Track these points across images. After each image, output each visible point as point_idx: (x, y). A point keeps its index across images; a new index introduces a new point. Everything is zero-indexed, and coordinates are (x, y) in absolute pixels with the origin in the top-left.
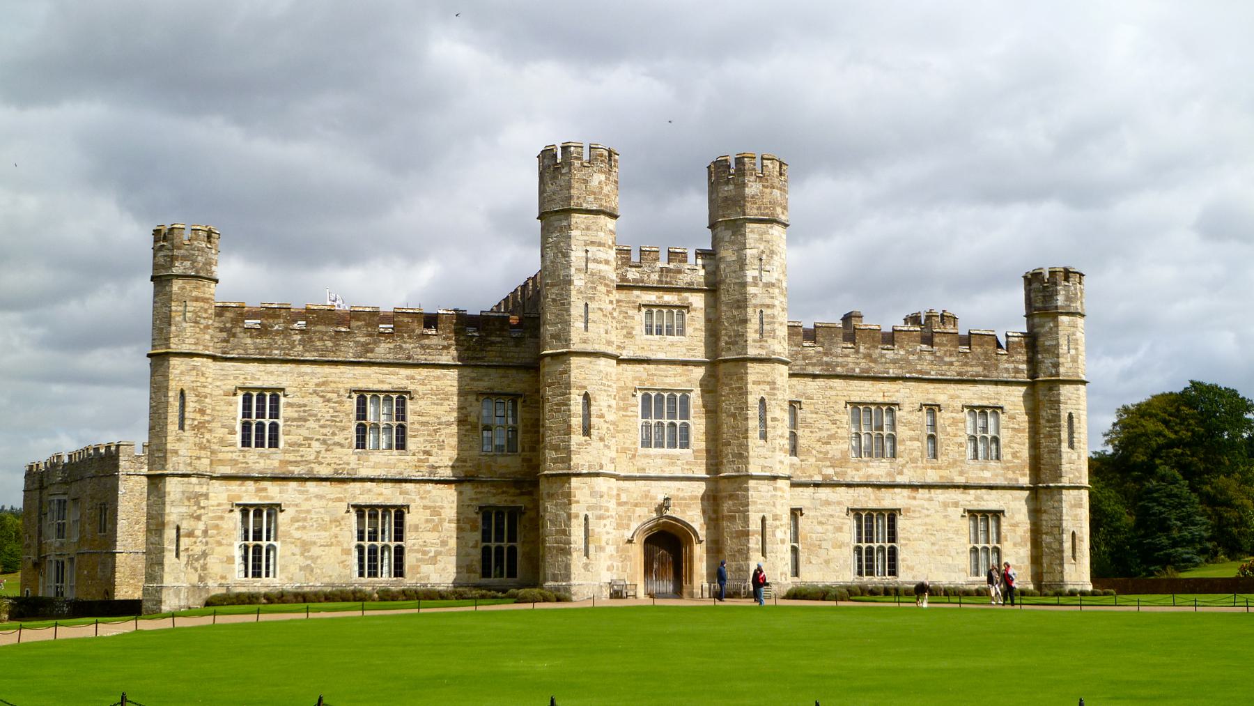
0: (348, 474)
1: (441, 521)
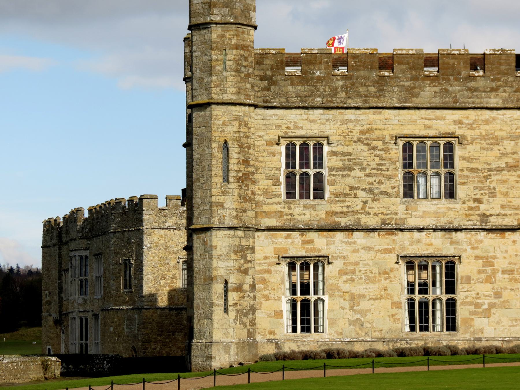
0: (396, 224)
1: (495, 272)
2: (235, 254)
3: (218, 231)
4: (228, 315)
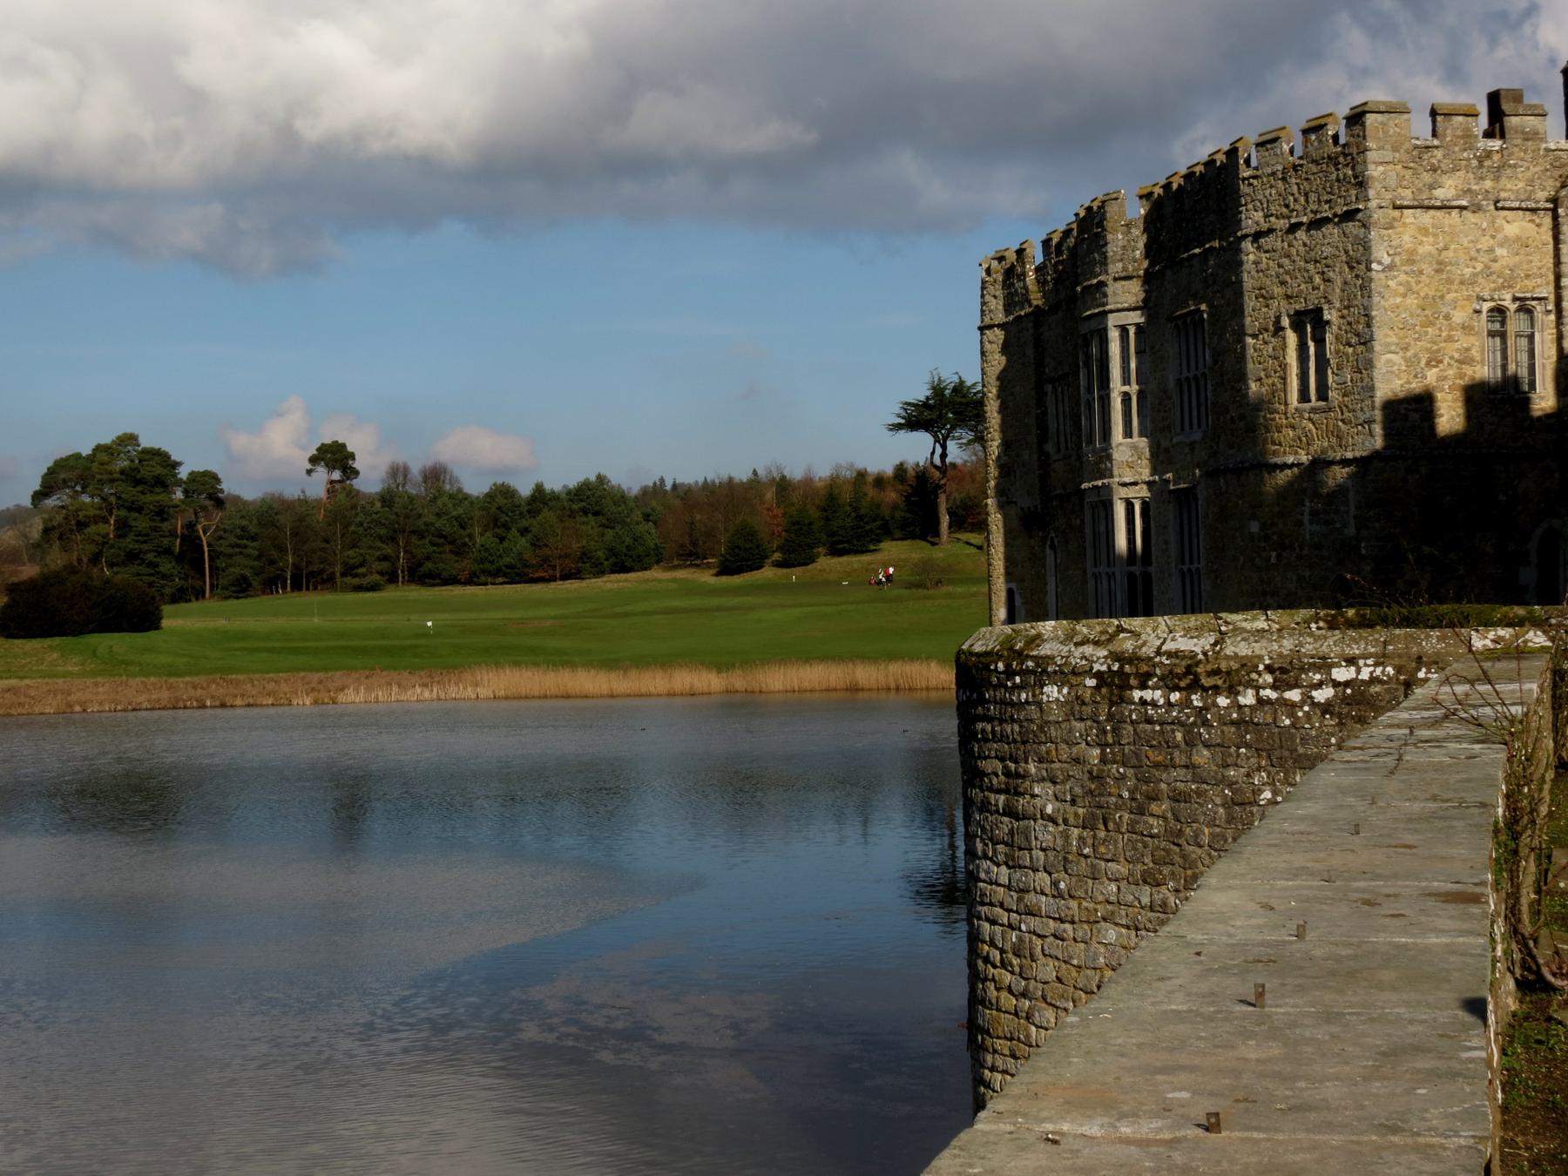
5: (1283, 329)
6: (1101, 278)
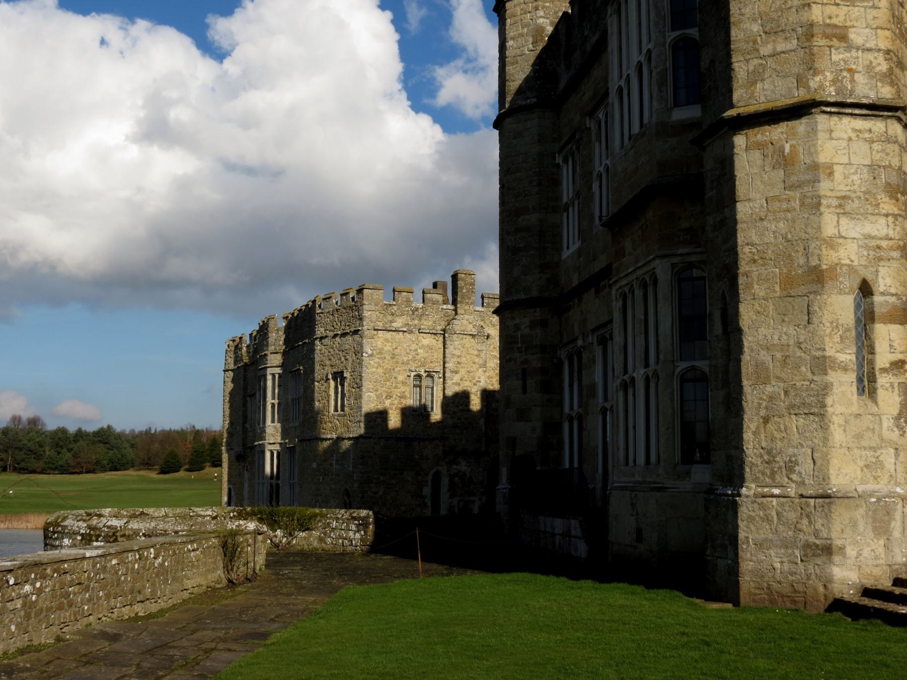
2: (891, 197)
3: (835, 119)
4: (876, 403)
5: (329, 379)
6: (266, 352)
